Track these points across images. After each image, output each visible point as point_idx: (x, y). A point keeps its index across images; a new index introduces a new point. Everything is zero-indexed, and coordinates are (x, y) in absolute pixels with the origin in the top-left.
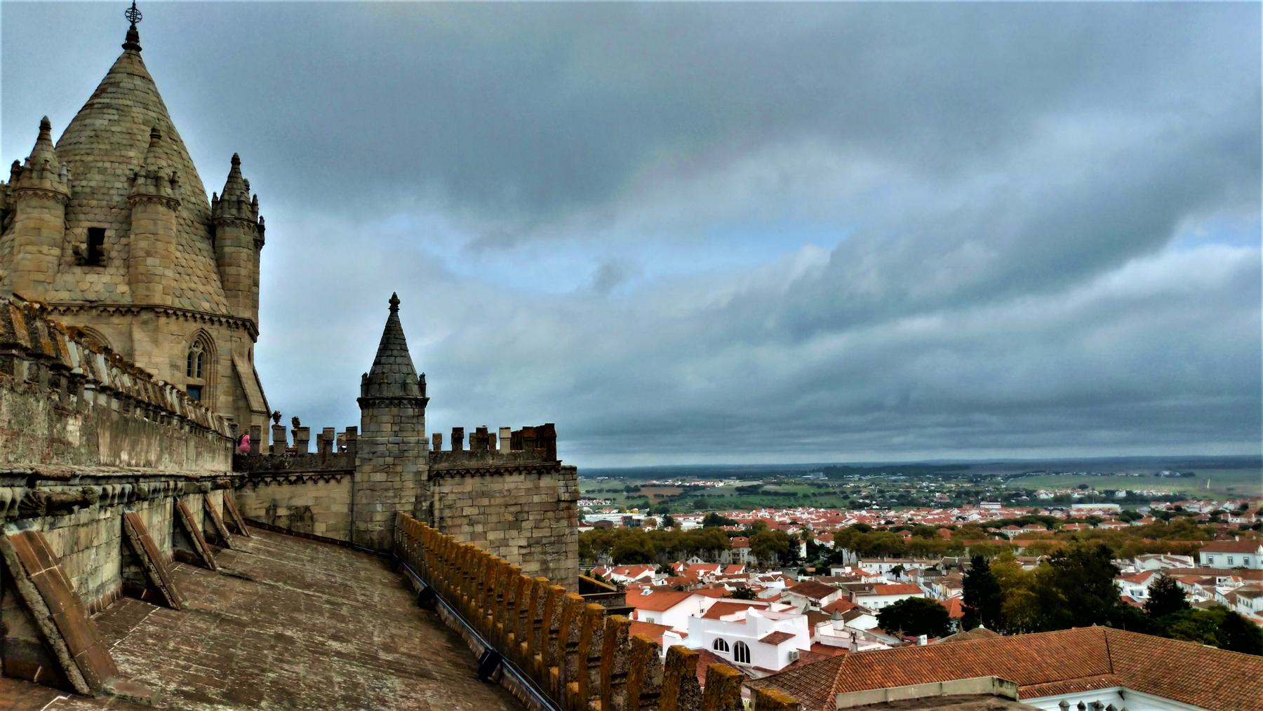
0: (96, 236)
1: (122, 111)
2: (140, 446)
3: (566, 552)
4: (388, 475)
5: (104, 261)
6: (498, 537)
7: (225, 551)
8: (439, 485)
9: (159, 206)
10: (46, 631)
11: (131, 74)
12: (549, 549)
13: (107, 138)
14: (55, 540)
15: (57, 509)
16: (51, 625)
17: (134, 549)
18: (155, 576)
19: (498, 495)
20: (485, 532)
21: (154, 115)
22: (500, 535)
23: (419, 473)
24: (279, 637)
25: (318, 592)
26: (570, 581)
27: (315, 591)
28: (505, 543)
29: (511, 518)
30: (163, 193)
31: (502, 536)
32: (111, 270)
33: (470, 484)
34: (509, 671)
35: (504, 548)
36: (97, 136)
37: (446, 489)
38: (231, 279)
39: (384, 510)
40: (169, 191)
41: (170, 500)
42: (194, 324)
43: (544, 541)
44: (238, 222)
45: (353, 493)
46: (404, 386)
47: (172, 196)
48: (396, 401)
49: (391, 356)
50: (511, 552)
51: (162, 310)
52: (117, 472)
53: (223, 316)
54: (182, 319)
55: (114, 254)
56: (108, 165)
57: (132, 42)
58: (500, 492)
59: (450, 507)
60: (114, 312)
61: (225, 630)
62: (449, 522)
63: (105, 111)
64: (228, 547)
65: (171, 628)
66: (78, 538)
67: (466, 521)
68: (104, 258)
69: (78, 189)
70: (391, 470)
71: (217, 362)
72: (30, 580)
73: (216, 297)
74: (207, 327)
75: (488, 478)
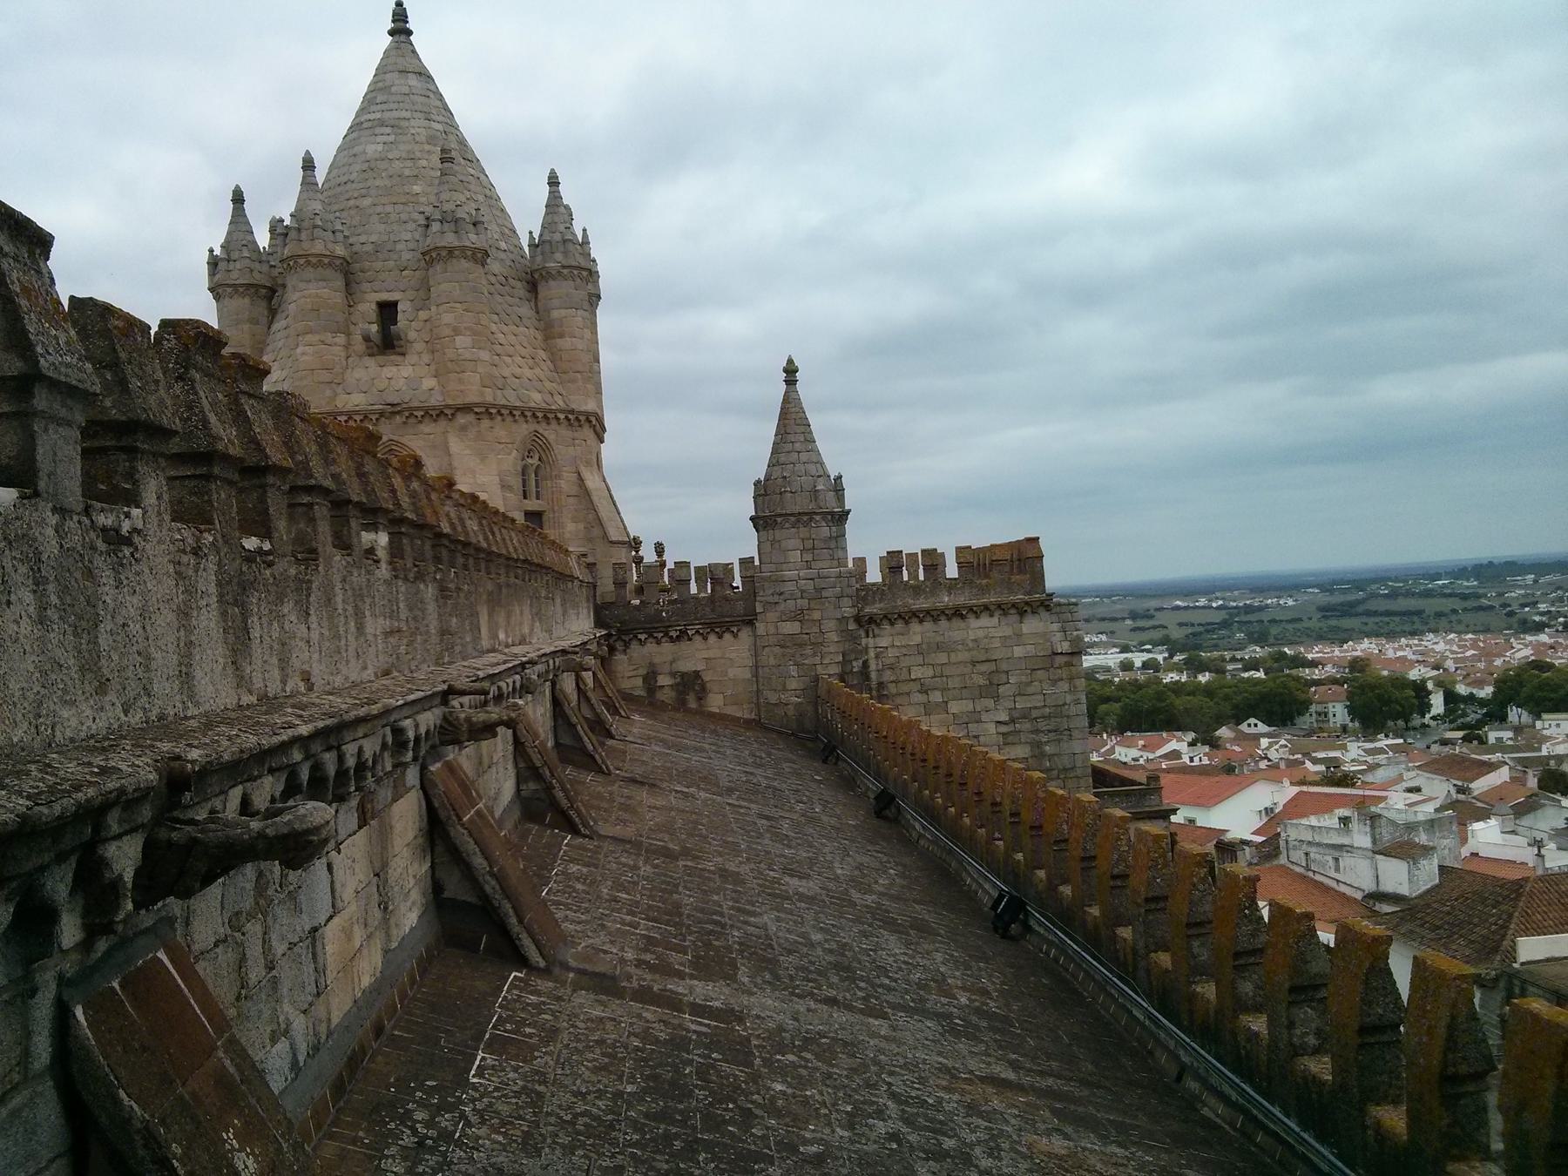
0: (388, 311)
2: (513, 618)
6: (965, 710)
7: (610, 742)
8: (874, 636)
9: (463, 261)
10: (487, 888)
12: (1042, 725)
16: (493, 882)
17: (531, 761)
18: (560, 795)
21: (439, 127)
22: (966, 706)
24: (724, 874)
26: (1079, 772)
27: (739, 798)
29: (982, 681)
31: (971, 707)
32: (411, 358)
33: (918, 633)
34: (1040, 924)
35: (976, 725)
37: (884, 642)
40: (473, 237)
42: (525, 426)
43: (1035, 714)
44: (565, 271)
48: (805, 518)
51: (483, 410)
53: (562, 411)
54: (509, 419)
55: (412, 335)
56: (389, 209)
57: (400, 28)
60: (422, 416)
61: (656, 867)
62: (892, 689)
63: (378, 130)
65: (596, 866)
67: (915, 686)
68: (402, 343)
69: (357, 248)
70: (806, 617)
73: (547, 384)
75: (943, 623)
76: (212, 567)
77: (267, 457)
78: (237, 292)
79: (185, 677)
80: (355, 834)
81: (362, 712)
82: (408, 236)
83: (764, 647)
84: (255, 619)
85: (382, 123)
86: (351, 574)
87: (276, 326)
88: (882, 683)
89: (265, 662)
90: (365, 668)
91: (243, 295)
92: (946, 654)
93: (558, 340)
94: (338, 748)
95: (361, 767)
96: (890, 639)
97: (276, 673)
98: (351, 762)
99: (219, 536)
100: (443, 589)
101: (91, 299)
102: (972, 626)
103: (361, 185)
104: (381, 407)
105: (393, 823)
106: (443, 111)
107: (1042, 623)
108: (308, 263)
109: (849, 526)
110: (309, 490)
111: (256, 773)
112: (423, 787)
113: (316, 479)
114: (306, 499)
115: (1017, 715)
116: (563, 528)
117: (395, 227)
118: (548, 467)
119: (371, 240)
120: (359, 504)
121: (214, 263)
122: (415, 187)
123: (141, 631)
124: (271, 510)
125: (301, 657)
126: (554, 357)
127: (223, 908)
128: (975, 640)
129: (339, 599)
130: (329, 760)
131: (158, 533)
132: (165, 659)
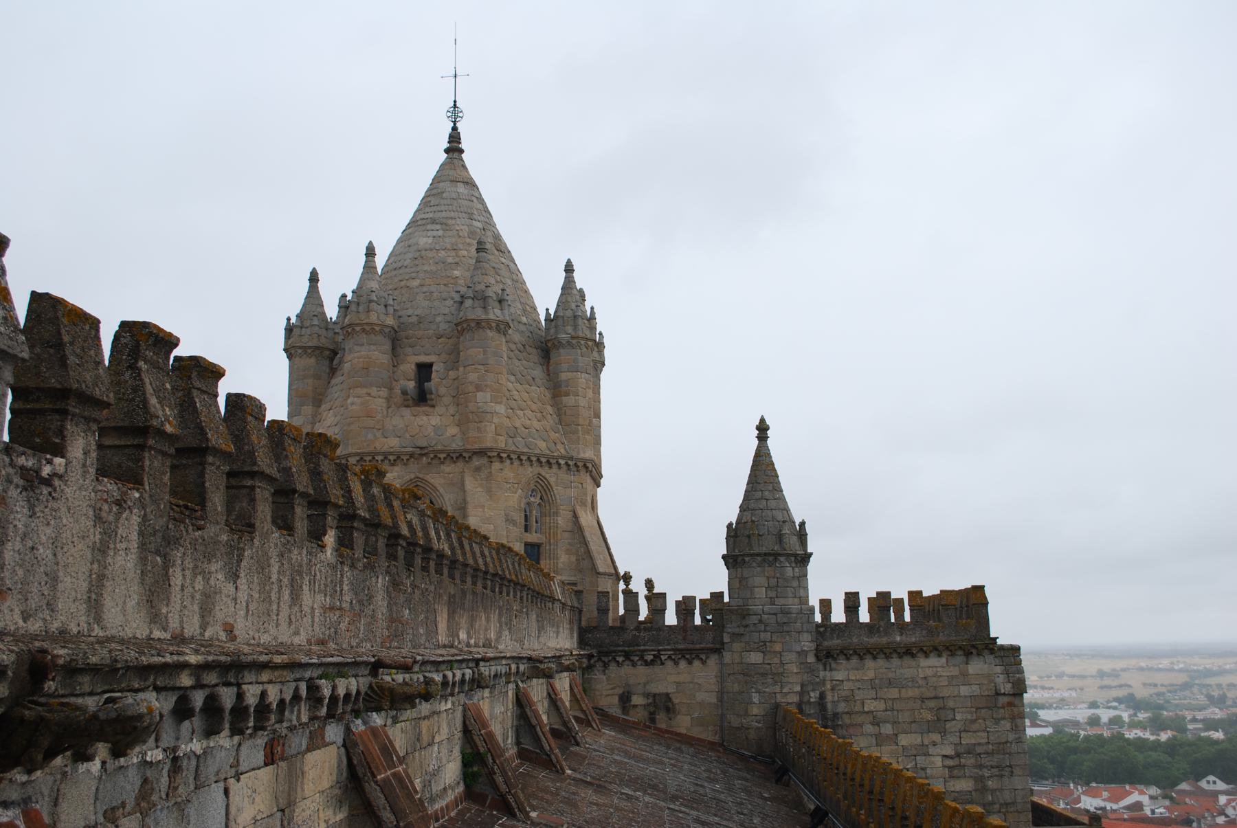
0: (424, 370)
1: (446, 225)
3: (1010, 766)
4: (764, 655)
5: (432, 400)
8: (831, 670)
9: (488, 331)
12: (986, 761)
13: (431, 258)
14: (399, 737)
15: (398, 700)
17: (477, 746)
18: (499, 779)
19: (910, 684)
20: (896, 735)
21: (479, 225)
23: (802, 653)
25: (685, 806)
26: (1019, 807)
28: (923, 750)
29: (929, 716)
32: (440, 409)
33: (872, 668)
35: (924, 758)
36: (422, 257)
37: (839, 675)
39: (763, 701)
40: (498, 312)
41: (512, 686)
42: (530, 469)
43: (979, 750)
44: (574, 341)
45: (721, 678)
46: (780, 537)
47: (501, 318)
48: (771, 558)
49: (762, 498)
50: (933, 763)
51: (496, 454)
52: (457, 655)
53: (562, 457)
54: (516, 463)
55: (442, 390)
57: (454, 147)
58: (913, 680)
59: (846, 699)
60: (445, 458)
63: (429, 227)
64: (578, 744)
66: (420, 733)
67: (869, 718)
68: (433, 396)
71: (557, 514)
72: (376, 782)
73: (552, 434)
74: (545, 471)
75: (895, 661)
76: (136, 519)
77: (207, 439)
79: (95, 606)
80: (259, 768)
81: (263, 658)
82: (447, 311)
83: (729, 675)
84: (178, 570)
85: (434, 221)
86: (290, 551)
87: (333, 382)
88: (838, 714)
89: (185, 607)
90: (297, 633)
91: (310, 356)
92: (896, 690)
93: (563, 398)
94: (239, 685)
95: (263, 708)
96: (847, 673)
97: (196, 620)
98: (251, 700)
99: (146, 496)
100: (395, 584)
101: (47, 294)
102: (922, 665)
103: (412, 270)
104: (411, 449)
105: (306, 769)
106: (483, 212)
107: (986, 666)
108: (364, 330)
109: (812, 567)
110: (253, 475)
111: (137, 686)
112: (344, 745)
113: (259, 466)
114: (249, 483)
115: (963, 751)
116: (557, 559)
117: (436, 303)
118: (547, 505)
119: (416, 313)
120: (304, 495)
121: (289, 330)
122: (455, 272)
123: (50, 556)
124: (207, 484)
125: (223, 610)
126: (560, 412)
127: (96, 799)
128: (925, 678)
129: (275, 569)
130: (227, 697)
131: (81, 481)
132: (73, 583)
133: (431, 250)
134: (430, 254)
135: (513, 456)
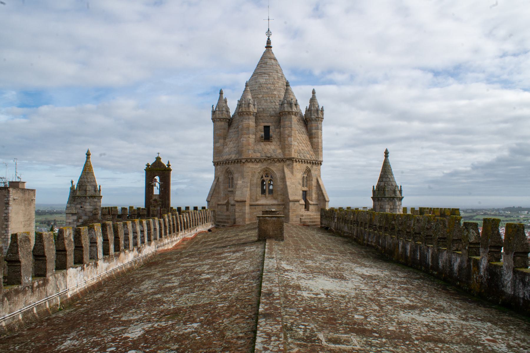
0: (267, 129)
1: (269, 75)
11: (271, 58)
30: (293, 110)
32: (274, 143)
38: (315, 144)
40: (295, 109)
44: (317, 119)
46: (395, 192)
47: (296, 111)
48: (392, 199)
53: (314, 160)
54: (301, 163)
55: (274, 136)
56: (268, 98)
57: (269, 46)
63: (263, 75)
71: (312, 180)
78: (220, 120)
85: (265, 73)
87: (230, 131)
91: (221, 121)
108: (247, 114)
121: (214, 112)
126: (312, 144)
133: (265, 84)
134: (265, 86)
135: (300, 160)
